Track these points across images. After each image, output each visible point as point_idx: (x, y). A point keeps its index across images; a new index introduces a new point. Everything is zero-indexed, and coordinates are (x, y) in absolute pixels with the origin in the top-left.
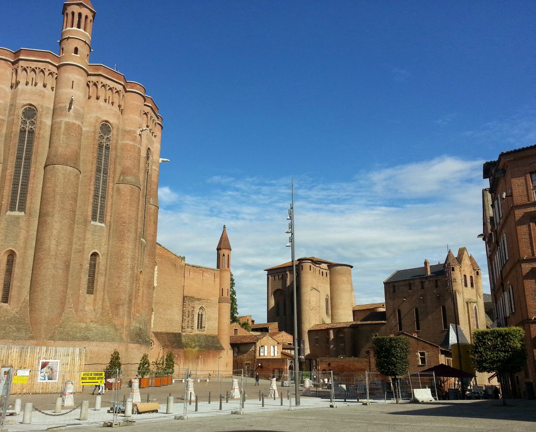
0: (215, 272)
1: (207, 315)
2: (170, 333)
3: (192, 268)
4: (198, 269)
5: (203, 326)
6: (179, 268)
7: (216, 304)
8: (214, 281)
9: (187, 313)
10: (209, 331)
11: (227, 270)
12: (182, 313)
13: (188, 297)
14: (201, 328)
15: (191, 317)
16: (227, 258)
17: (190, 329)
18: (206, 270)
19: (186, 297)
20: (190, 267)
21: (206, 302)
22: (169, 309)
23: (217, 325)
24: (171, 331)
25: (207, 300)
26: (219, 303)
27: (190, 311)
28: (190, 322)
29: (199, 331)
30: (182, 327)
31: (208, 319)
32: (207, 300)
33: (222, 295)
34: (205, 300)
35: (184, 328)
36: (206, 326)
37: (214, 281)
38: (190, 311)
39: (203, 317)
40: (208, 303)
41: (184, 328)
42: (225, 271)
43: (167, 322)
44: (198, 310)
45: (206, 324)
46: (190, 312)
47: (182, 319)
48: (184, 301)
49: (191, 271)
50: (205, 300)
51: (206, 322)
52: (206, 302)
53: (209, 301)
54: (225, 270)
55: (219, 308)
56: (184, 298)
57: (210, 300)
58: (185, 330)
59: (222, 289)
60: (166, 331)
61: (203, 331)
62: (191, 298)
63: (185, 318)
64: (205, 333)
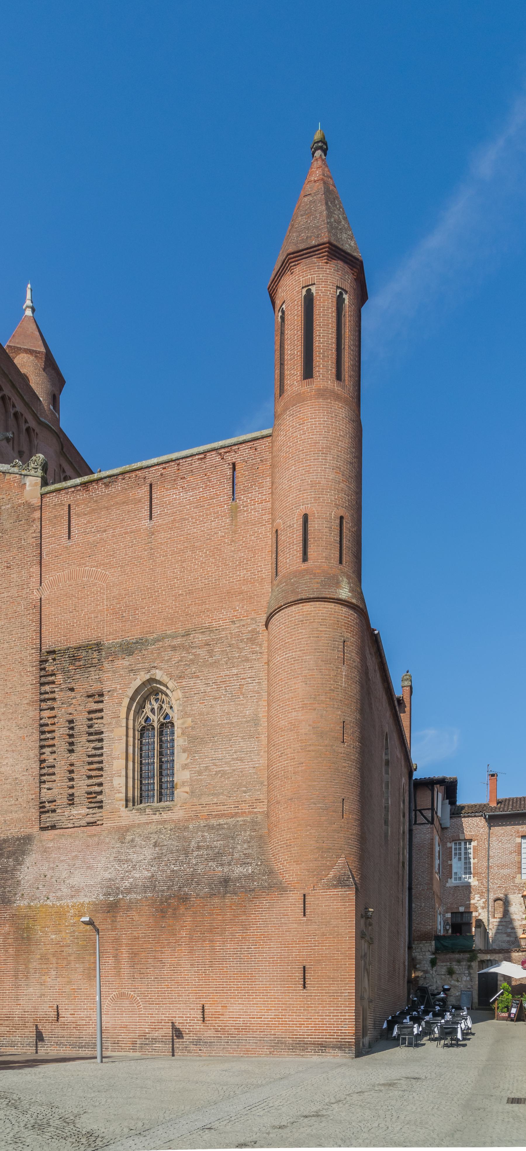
9: (61, 730)
10: (204, 800)
12: (36, 736)
17: (84, 811)
21: (174, 648)
31: (193, 740)
34: (174, 637)
40: (187, 649)
45: (185, 767)
46: (81, 726)
50: (174, 637)
52: (174, 648)
61: (169, 809)
63: (50, 760)
64: (178, 813)
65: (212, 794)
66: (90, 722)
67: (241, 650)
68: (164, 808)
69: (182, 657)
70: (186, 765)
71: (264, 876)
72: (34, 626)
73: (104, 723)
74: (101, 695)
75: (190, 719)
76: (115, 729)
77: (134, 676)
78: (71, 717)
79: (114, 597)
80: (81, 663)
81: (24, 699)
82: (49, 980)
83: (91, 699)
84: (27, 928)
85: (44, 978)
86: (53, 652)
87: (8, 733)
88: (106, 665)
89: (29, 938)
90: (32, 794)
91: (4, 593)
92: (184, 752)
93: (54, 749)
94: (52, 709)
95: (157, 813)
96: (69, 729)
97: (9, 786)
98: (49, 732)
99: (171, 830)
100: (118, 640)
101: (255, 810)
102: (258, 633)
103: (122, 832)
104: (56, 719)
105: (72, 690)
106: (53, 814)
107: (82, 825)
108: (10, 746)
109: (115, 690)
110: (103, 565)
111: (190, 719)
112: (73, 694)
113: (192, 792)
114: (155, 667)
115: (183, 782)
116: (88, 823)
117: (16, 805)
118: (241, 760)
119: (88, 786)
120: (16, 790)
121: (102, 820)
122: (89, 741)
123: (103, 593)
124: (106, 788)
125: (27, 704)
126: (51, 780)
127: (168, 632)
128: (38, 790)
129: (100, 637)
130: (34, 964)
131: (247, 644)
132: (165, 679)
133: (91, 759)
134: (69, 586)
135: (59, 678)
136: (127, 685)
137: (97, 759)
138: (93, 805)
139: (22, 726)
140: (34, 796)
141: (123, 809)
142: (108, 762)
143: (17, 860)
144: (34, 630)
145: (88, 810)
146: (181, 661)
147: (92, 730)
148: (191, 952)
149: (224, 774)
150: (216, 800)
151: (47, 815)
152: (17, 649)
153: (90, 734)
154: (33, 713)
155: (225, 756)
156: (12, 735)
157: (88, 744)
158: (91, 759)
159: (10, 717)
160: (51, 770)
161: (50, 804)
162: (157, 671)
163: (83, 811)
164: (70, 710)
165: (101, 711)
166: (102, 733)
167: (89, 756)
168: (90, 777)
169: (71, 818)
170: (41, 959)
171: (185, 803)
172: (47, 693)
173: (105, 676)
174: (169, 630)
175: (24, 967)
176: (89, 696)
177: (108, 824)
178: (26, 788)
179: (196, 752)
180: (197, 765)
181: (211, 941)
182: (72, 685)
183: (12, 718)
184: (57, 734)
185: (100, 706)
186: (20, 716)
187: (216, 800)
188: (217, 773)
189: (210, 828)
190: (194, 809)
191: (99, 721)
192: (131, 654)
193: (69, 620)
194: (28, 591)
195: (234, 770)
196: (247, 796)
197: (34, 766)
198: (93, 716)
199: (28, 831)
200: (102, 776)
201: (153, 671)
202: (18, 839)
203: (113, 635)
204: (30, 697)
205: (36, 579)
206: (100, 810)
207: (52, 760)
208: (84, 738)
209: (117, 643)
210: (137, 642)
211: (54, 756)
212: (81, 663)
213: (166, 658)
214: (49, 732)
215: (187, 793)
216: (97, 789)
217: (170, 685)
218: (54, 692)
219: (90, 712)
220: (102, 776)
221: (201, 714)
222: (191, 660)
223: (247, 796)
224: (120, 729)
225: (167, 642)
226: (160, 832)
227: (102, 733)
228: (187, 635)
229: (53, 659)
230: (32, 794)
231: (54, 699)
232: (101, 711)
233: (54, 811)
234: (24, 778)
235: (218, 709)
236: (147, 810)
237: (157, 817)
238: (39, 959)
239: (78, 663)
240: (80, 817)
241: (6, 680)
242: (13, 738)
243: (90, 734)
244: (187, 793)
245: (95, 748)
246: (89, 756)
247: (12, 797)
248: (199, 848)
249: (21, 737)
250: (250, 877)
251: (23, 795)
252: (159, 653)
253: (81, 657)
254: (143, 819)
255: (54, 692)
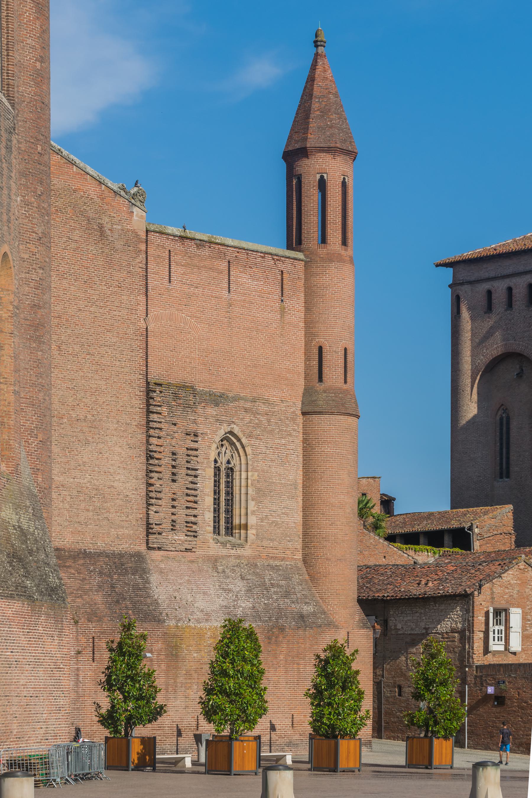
0: (287, 266)
1: (254, 470)
2: (100, 554)
3: (178, 246)
4: (206, 252)
5: (236, 521)
6: (119, 245)
7: (294, 420)
8: (283, 311)
9: (166, 460)
10: (265, 543)
11: (340, 259)
12: (143, 459)
13: (169, 385)
14: (230, 530)
15: (183, 480)
16: (339, 198)
17: (183, 537)
18: (242, 256)
19: (158, 389)
20: (169, 244)
21: (246, 410)
22: (87, 442)
23: (298, 517)
24: (101, 545)
25: (254, 401)
26: (304, 414)
27: (181, 451)
28: (182, 501)
29: (224, 544)
30: (148, 524)
31: (258, 490)
32: (254, 401)
33: (320, 379)
34: (245, 400)
35: (156, 528)
36: (252, 520)
37: (283, 311)
38: (181, 451)
39: (236, 483)
40: (255, 413)
41: (156, 528)
42: (331, 261)
43: (83, 505)
44: (214, 446)
45: (253, 512)
46: (181, 460)
47: (148, 492)
48: (148, 405)
49: (177, 264)
50: (245, 400)
51: (252, 506)
52: (246, 410)
53: (263, 408)
54: (331, 258)
55: (305, 441)
56: (149, 392)
57: (267, 402)
58: (161, 539)
59: (320, 349)
60: (81, 546)
61: (241, 546)
62: (182, 393)
64: (247, 552)
65: (271, 540)
66: (189, 458)
67: (287, 426)
68: (239, 545)
69: (251, 419)
70: (254, 511)
71: (322, 615)
72: (142, 354)
73: (199, 461)
74: (196, 435)
75: (256, 474)
76: (206, 469)
77: (220, 426)
78: (173, 449)
79: (204, 350)
80: (181, 401)
81: (133, 420)
82: (192, 693)
83: (188, 437)
84: (175, 646)
85: (188, 691)
86: (160, 385)
87: (120, 450)
88: (200, 410)
89: (177, 656)
90: (140, 514)
91: (115, 311)
92: (253, 500)
93: (161, 475)
94: (159, 438)
95: (234, 548)
96: (172, 460)
97: (121, 502)
98: (157, 459)
99: (246, 565)
100: (206, 389)
101: (295, 557)
102: (296, 415)
103: (214, 561)
104: (162, 448)
105: (175, 424)
106: (159, 536)
107: (182, 550)
108: (121, 463)
109: (206, 434)
110: (196, 317)
111: (256, 474)
112: (175, 428)
113: (257, 535)
114: (233, 422)
115: (252, 526)
116: (186, 549)
117: (127, 521)
118: (287, 514)
119: (186, 515)
120: (126, 506)
121: (196, 548)
122: (187, 475)
123: (195, 342)
124: (199, 519)
125: (136, 426)
126: (157, 504)
127: (242, 395)
128: (145, 510)
129: (193, 381)
130: (181, 679)
131: (290, 422)
132: (240, 435)
133: (189, 492)
134: (170, 326)
135: (164, 410)
136: (215, 432)
137: (193, 492)
138: (189, 533)
139: (131, 446)
140: (141, 516)
141: (211, 541)
142: (201, 497)
143: (141, 577)
144: (142, 357)
145: (186, 537)
146: (250, 423)
147: (189, 466)
148: (286, 672)
149: (277, 524)
150: (271, 544)
151: (155, 536)
152: (126, 370)
153: (188, 468)
154: (141, 436)
155: (277, 510)
156: (124, 453)
157: (187, 477)
158: (189, 492)
159: (122, 434)
160: (159, 495)
161: (157, 527)
162: (235, 426)
163: (183, 538)
164: (174, 442)
165: (196, 450)
166: (197, 470)
167: (187, 488)
168: (187, 508)
169: (173, 542)
170: (186, 675)
171: (253, 543)
172: (156, 422)
173: (201, 419)
174: (242, 393)
175: (173, 681)
176: (187, 434)
177: (199, 552)
178: (135, 507)
179: (261, 502)
180: (260, 512)
181: (298, 664)
182: (175, 420)
183: (123, 436)
184: (162, 462)
185: (194, 445)
186: (130, 436)
187: (271, 544)
188: (273, 522)
189: (272, 568)
190: (258, 550)
191: (195, 458)
192: (217, 405)
193: (170, 357)
194: (136, 317)
195: (283, 522)
196: (290, 545)
197: (142, 487)
198: (190, 452)
199: (137, 548)
200: (196, 509)
201: (232, 426)
202: (132, 556)
203: (203, 383)
204: (139, 420)
205: (142, 308)
206: (196, 539)
207: (158, 486)
208: (183, 471)
209: (206, 391)
210: (221, 397)
211: (161, 482)
212: (181, 401)
213: (241, 417)
214: (157, 459)
215: (254, 535)
216: (193, 519)
217: (244, 440)
218: (160, 422)
219: (187, 449)
220: (196, 509)
221: (263, 471)
222: (256, 424)
223: (290, 545)
224: (210, 469)
225: (242, 403)
226: (240, 566)
227: (197, 470)
228: (255, 402)
229: (160, 391)
230: (140, 514)
231: (161, 429)
232: (196, 450)
233: (160, 534)
234: (133, 496)
235: (273, 470)
236: (228, 545)
237: (233, 552)
238: (184, 674)
239: (178, 401)
240: (180, 542)
241: (118, 397)
242: (124, 456)
243: (188, 468)
244: (254, 535)
245: (192, 483)
246: (187, 488)
247: (123, 513)
248: (272, 585)
249: (131, 456)
250: (314, 614)
251: (133, 513)
252: (236, 411)
253: (180, 395)
254: (224, 552)
255: (160, 422)
